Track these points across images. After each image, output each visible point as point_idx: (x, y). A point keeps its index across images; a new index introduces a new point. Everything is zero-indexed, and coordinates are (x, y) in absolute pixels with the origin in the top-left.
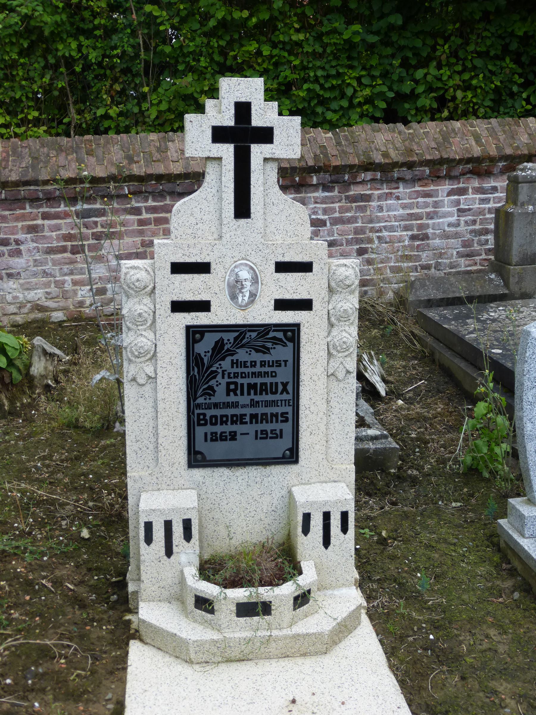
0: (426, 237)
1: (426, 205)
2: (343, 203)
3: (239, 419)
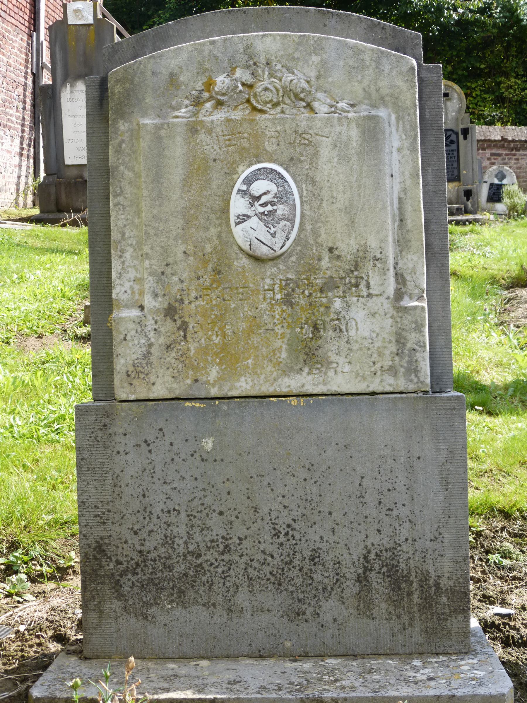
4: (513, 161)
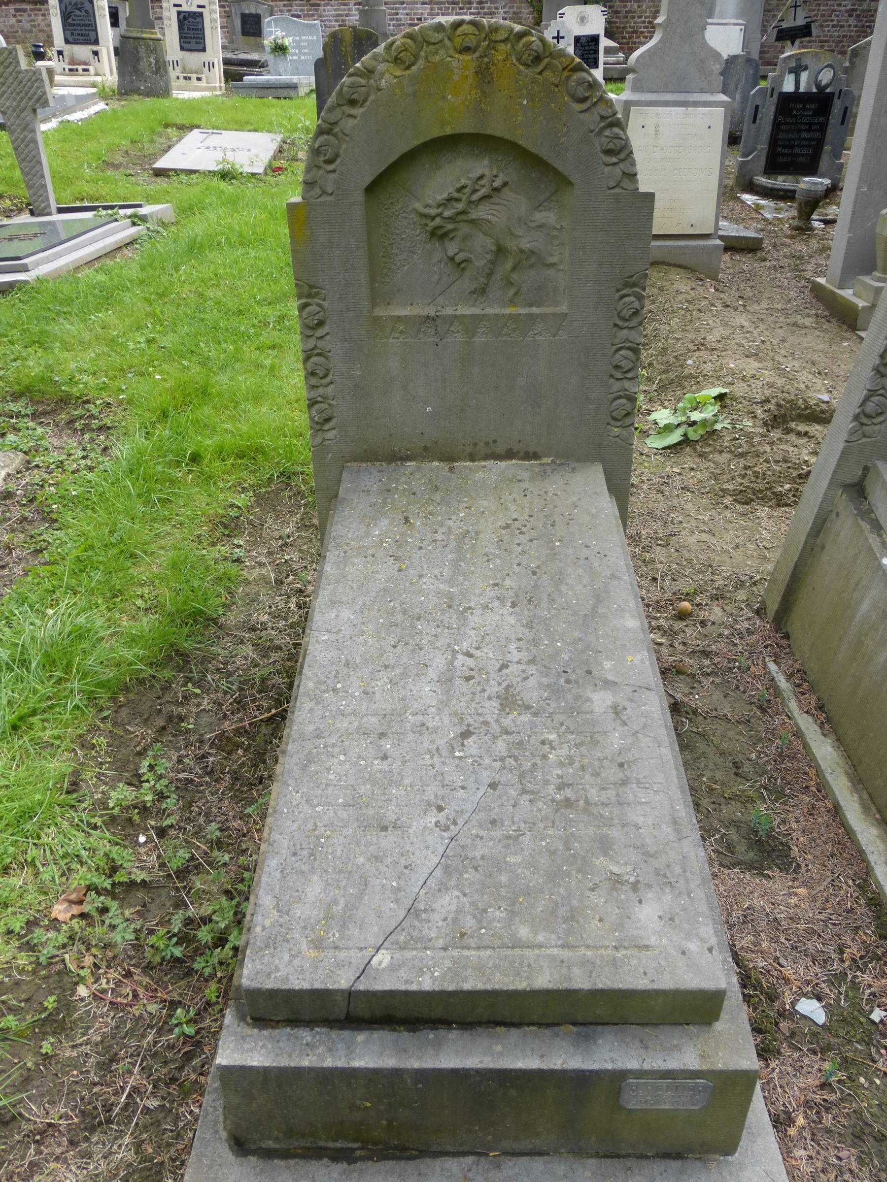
1: (345, 10)
2: (308, 7)
3: (191, 38)
4: (41, 18)
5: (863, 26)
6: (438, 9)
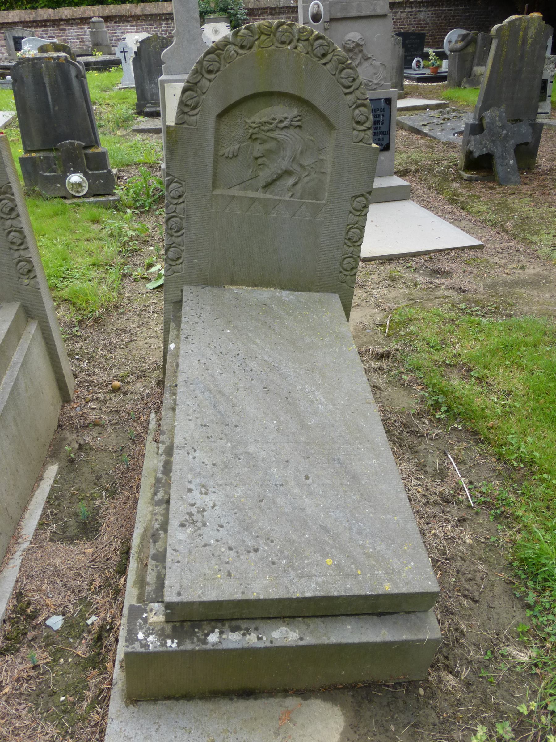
0: (84, 42)
1: (82, 32)
5: (398, 28)
6: (142, 28)
